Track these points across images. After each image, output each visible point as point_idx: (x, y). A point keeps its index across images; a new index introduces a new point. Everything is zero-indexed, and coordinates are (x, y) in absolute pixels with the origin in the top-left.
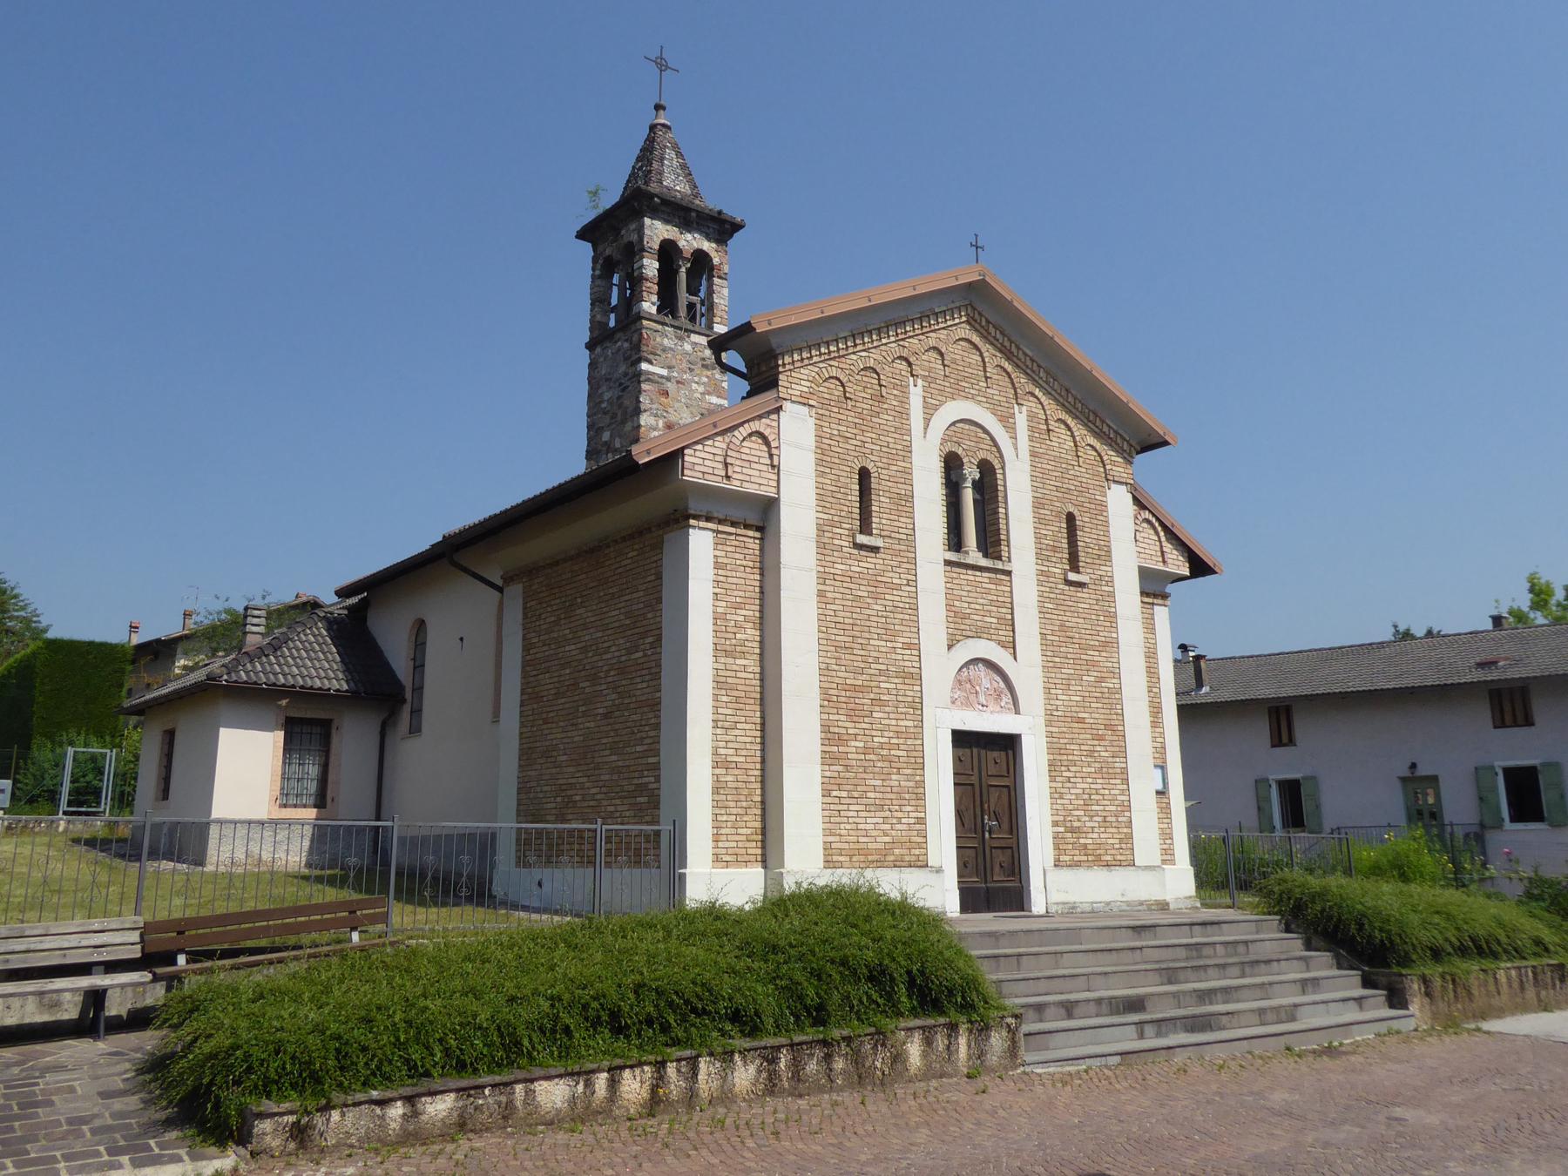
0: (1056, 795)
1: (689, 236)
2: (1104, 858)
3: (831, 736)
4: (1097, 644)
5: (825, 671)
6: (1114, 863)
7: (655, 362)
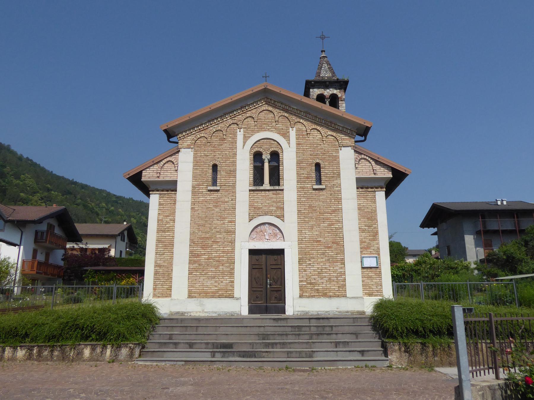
1: (328, 90)
4: (330, 211)
5: (192, 233)
6: (335, 296)
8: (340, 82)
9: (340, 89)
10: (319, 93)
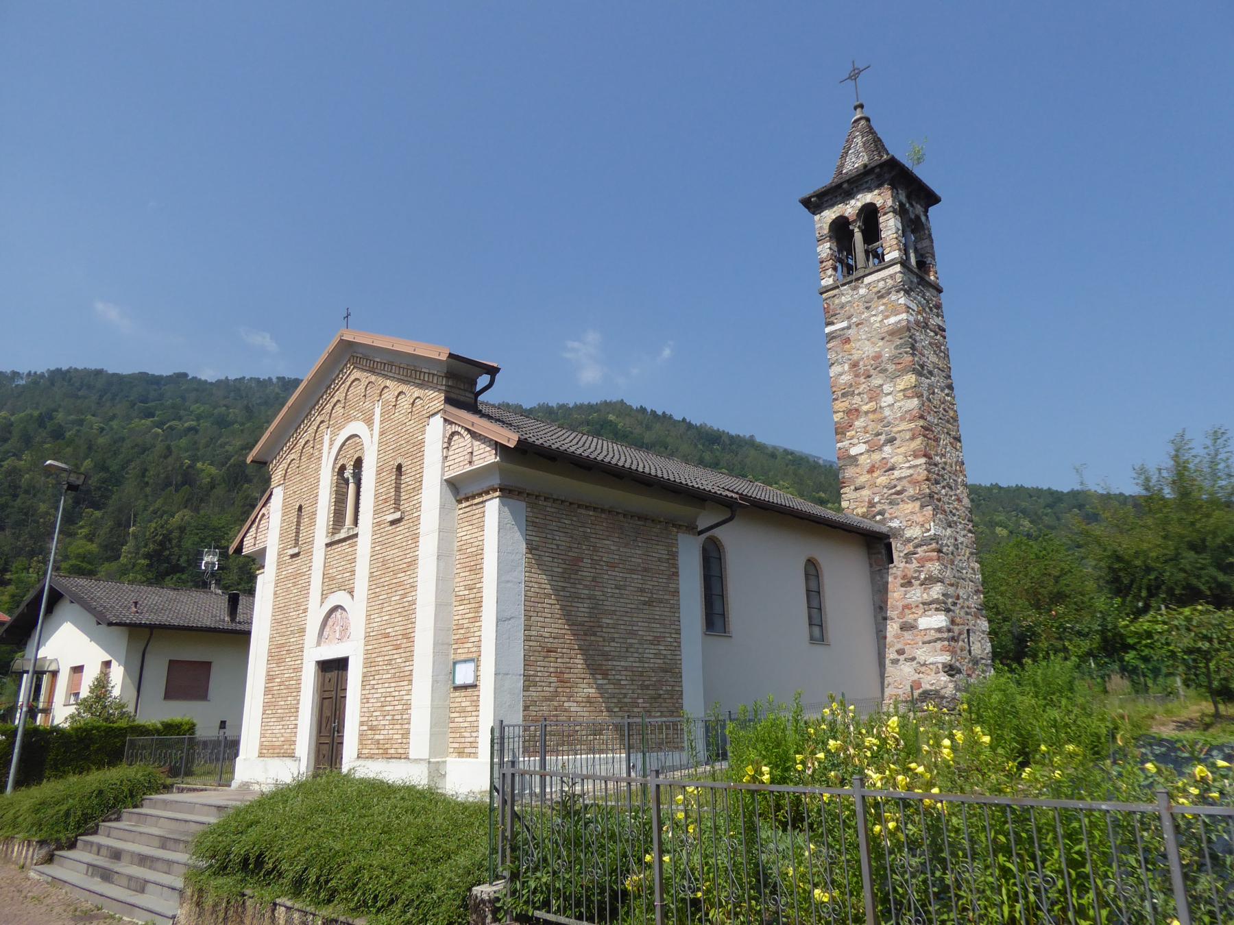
0: (365, 700)
1: (853, 202)
2: (390, 751)
3: (270, 678)
4: (405, 565)
5: (272, 638)
6: (396, 755)
7: (835, 321)
8: (873, 168)
9: (879, 186)
10: (834, 217)
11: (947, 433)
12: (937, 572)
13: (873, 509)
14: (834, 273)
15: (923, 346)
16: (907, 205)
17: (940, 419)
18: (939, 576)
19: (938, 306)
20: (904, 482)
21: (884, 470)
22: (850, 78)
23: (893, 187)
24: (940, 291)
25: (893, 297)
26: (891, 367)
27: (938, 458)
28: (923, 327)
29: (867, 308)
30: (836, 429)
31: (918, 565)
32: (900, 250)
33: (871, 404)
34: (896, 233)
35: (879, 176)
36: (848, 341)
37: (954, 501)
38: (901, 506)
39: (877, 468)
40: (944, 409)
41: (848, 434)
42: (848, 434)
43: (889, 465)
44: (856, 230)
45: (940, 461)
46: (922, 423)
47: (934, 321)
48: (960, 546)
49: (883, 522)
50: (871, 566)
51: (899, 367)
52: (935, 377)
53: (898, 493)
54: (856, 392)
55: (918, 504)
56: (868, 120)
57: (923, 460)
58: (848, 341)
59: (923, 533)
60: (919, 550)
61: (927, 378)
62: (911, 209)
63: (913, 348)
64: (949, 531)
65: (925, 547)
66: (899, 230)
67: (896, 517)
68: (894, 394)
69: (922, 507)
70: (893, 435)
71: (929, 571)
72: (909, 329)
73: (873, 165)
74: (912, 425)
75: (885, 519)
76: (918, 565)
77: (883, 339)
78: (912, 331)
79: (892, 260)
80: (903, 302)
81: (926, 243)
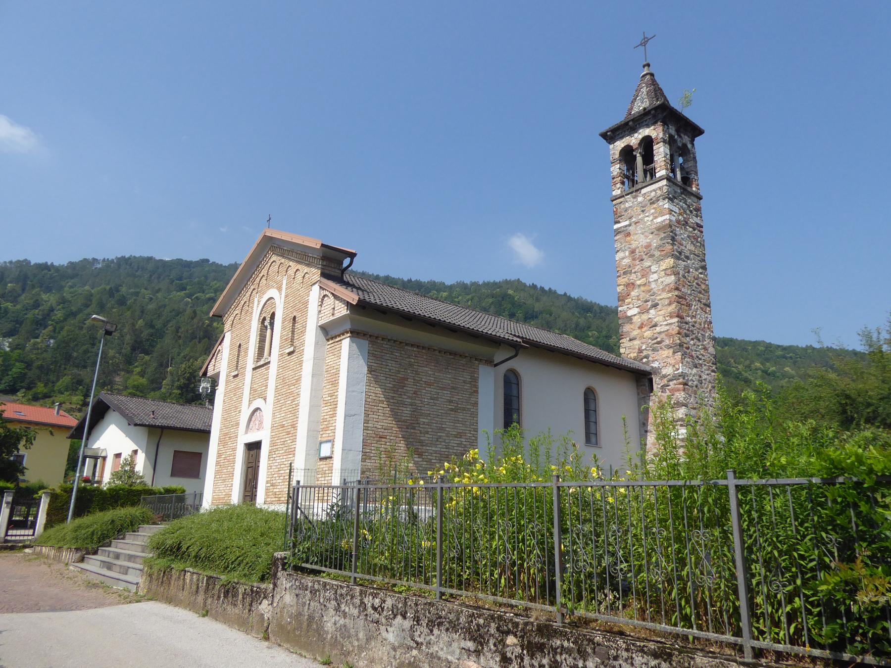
0: (270, 467)
1: (636, 135)
2: (281, 499)
3: (219, 455)
5: (221, 430)
7: (621, 220)
8: (650, 111)
9: (655, 123)
10: (623, 146)
11: (699, 301)
12: (682, 399)
13: (641, 354)
14: (622, 186)
15: (682, 238)
16: (676, 137)
17: (693, 290)
18: (684, 402)
19: (698, 210)
20: (663, 336)
21: (650, 326)
22: (641, 44)
23: (665, 123)
24: (700, 198)
25: (661, 203)
26: (657, 253)
27: (689, 319)
28: (684, 225)
29: (643, 211)
30: (619, 297)
31: (670, 394)
32: (667, 169)
33: (643, 279)
34: (665, 157)
35: (654, 116)
36: (629, 234)
37: (701, 349)
38: (660, 352)
39: (645, 325)
40: (697, 284)
41: (626, 301)
42: (626, 301)
43: (653, 323)
44: (638, 155)
45: (690, 320)
46: (676, 293)
47: (693, 220)
48: (703, 381)
49: (647, 363)
50: (638, 394)
51: (663, 253)
52: (691, 260)
53: (659, 343)
54: (633, 271)
55: (671, 351)
56: (652, 75)
57: (676, 320)
58: (629, 234)
59: (674, 371)
60: (671, 383)
61: (684, 261)
62: (679, 140)
63: (673, 239)
64: (695, 370)
65: (675, 381)
66: (667, 155)
67: (656, 360)
68: (658, 272)
69: (674, 353)
70: (656, 301)
71: (677, 398)
72: (670, 226)
73: (650, 108)
74: (670, 295)
75: (648, 362)
76: (670, 394)
77: (652, 233)
78: (673, 227)
79: (661, 176)
80: (667, 207)
81: (691, 164)
